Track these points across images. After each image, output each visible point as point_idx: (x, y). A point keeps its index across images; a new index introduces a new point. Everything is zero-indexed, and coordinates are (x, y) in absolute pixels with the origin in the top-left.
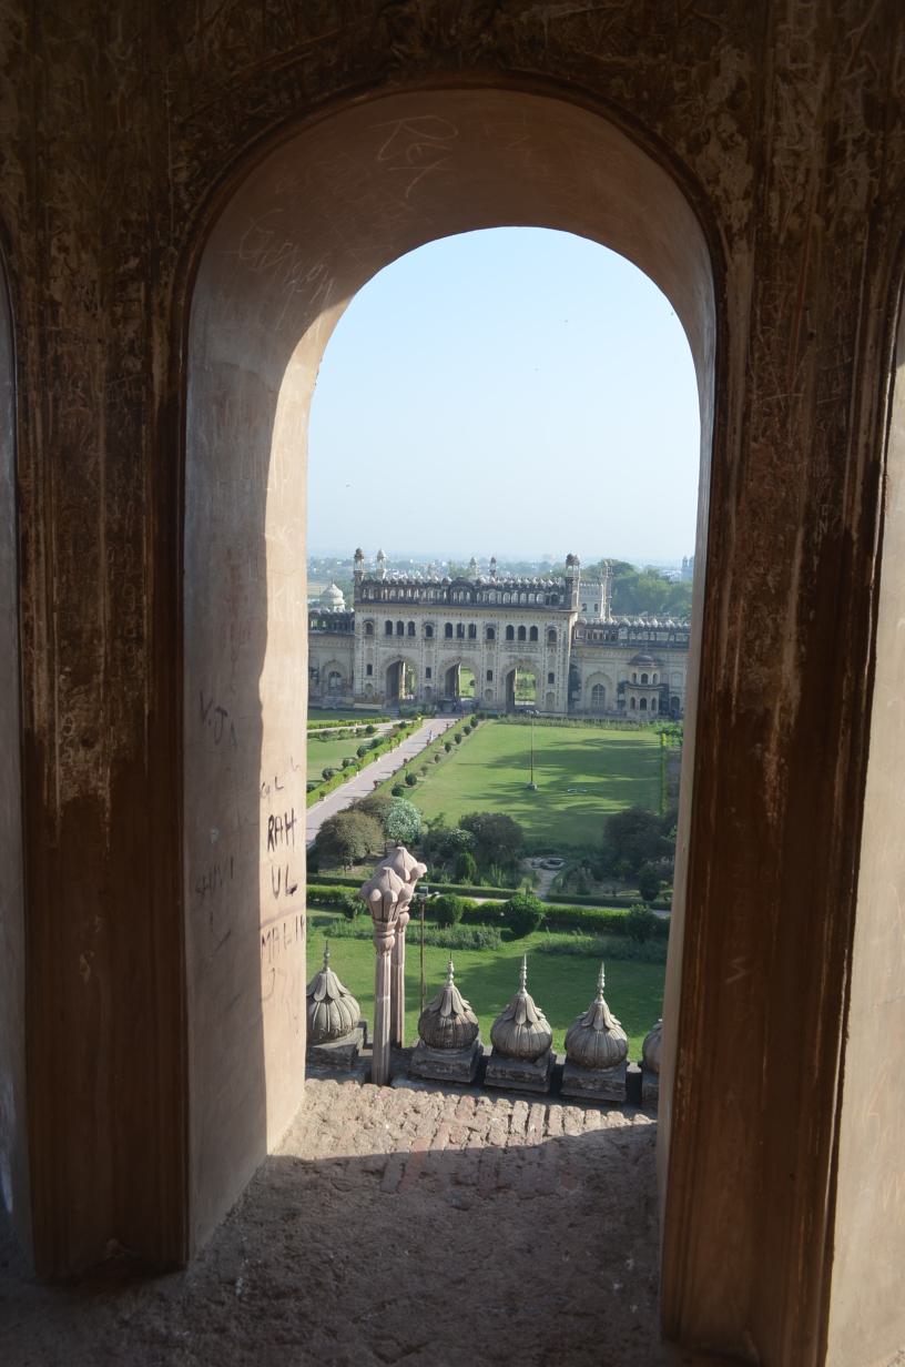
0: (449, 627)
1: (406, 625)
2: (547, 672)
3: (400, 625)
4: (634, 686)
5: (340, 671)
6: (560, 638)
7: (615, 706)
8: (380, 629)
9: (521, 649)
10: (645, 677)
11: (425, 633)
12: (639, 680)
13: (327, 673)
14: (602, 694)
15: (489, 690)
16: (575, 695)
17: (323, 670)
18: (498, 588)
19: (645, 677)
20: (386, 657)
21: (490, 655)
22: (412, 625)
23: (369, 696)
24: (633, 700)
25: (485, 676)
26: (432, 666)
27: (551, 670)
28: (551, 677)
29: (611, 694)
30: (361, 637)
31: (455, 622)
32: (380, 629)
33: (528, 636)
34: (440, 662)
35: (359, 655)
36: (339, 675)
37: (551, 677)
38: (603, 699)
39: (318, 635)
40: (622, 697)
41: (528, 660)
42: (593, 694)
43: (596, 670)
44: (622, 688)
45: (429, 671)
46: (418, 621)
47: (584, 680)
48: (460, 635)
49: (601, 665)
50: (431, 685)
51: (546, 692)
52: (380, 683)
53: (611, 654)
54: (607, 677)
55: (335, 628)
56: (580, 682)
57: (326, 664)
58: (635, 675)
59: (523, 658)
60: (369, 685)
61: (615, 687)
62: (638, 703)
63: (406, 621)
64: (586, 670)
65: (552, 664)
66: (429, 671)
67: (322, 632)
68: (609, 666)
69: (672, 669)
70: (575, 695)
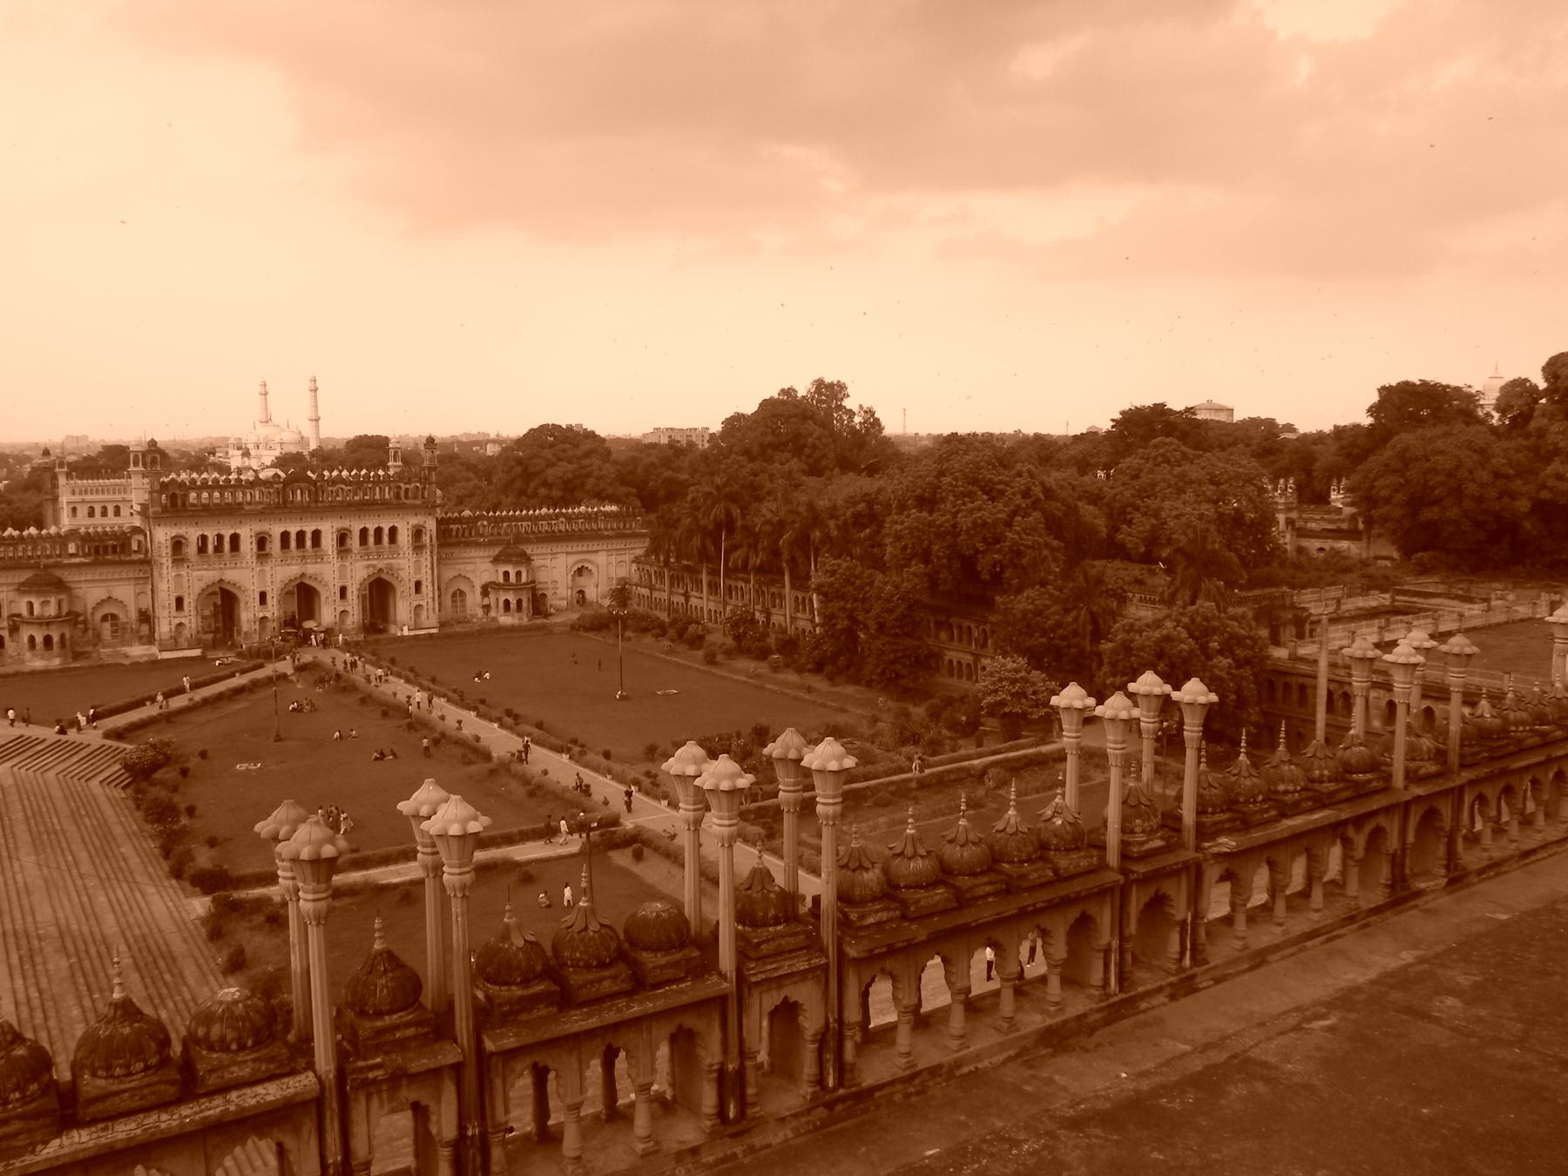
0: (285, 536)
1: (227, 539)
3: (220, 537)
4: (506, 585)
6: (426, 539)
7: (480, 612)
8: (191, 550)
9: (379, 555)
10: (519, 574)
12: (512, 578)
13: (98, 616)
14: (463, 601)
19: (519, 574)
20: (203, 585)
21: (342, 567)
22: (235, 539)
23: (182, 640)
24: (507, 602)
26: (268, 589)
27: (418, 577)
28: (418, 585)
29: (474, 600)
31: (293, 529)
32: (191, 550)
33: (386, 539)
34: (278, 585)
36: (114, 617)
37: (418, 585)
40: (486, 601)
41: (390, 568)
42: (454, 601)
44: (485, 591)
45: (263, 596)
46: (247, 533)
50: (268, 615)
52: (191, 620)
53: (474, 553)
55: (106, 552)
58: (506, 574)
60: (180, 624)
61: (478, 590)
62: (513, 605)
63: (227, 533)
65: (418, 570)
66: (263, 596)
68: (469, 567)
69: (537, 562)
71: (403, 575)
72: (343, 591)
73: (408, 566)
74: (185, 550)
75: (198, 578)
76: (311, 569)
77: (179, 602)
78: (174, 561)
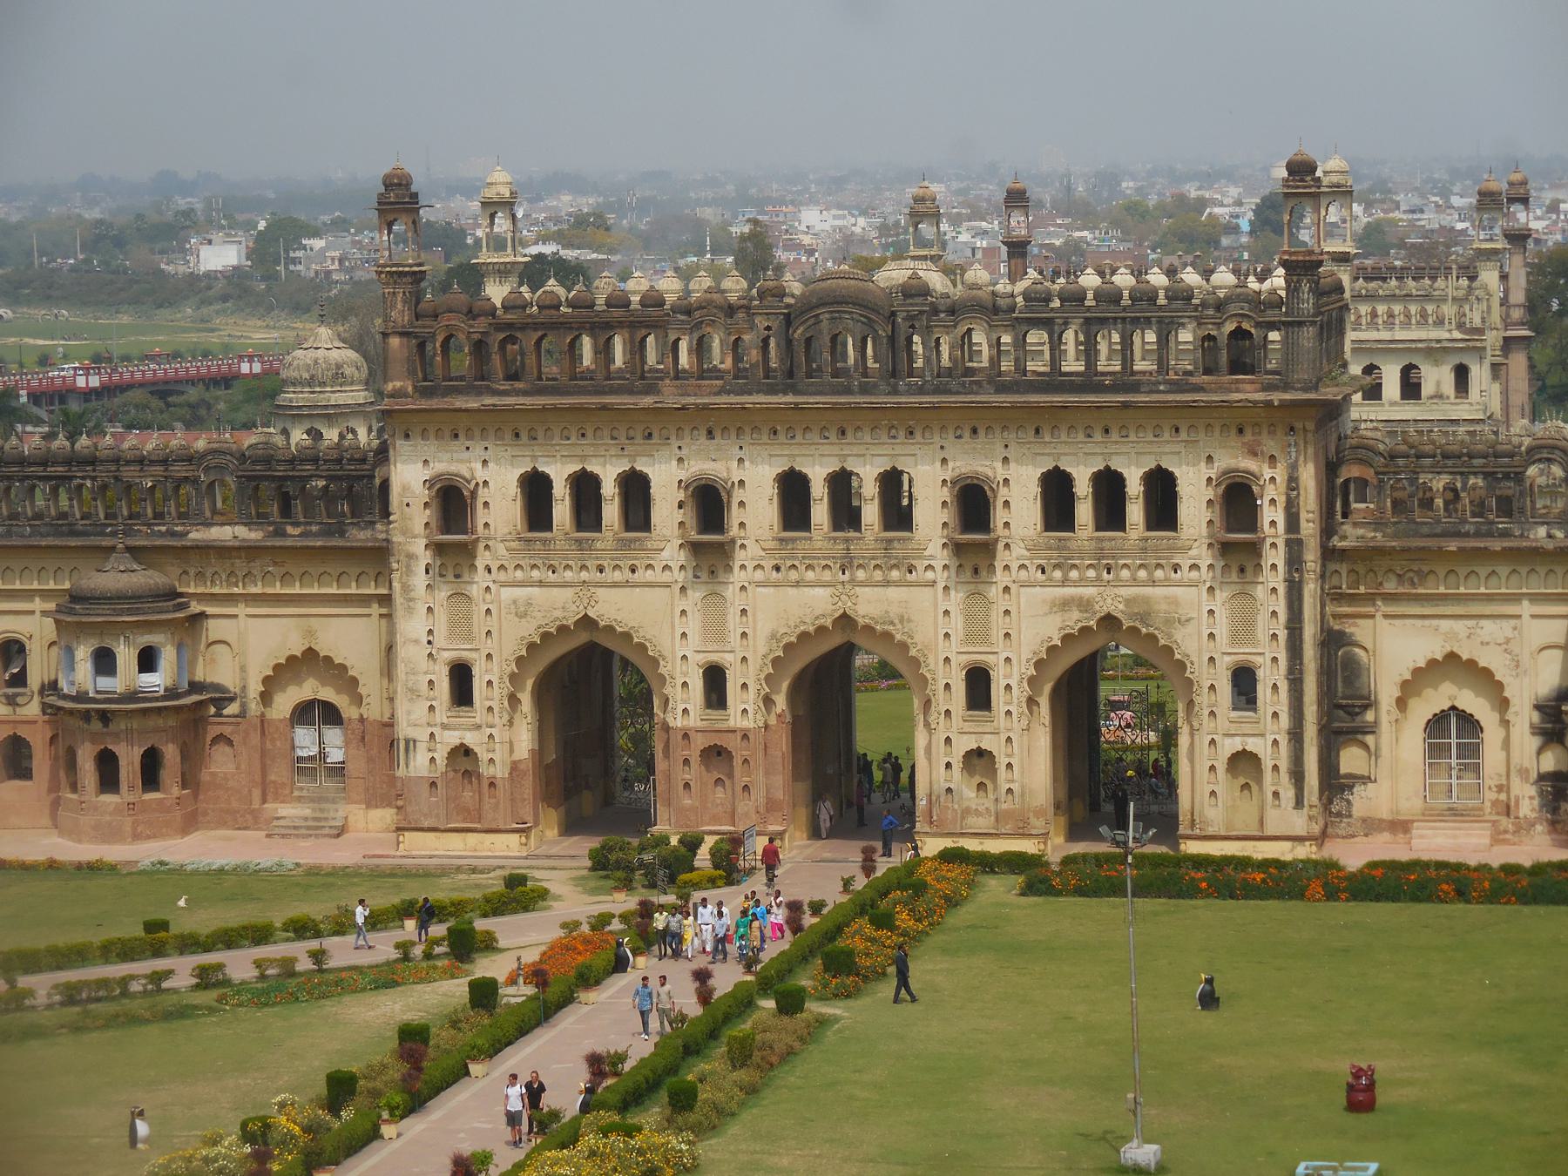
1: (609, 488)
2: (1225, 664)
5: (327, 694)
6: (1271, 515)
11: (689, 516)
15: (980, 753)
16: (1350, 760)
17: (266, 698)
18: (992, 310)
20: (529, 630)
25: (959, 689)
26: (726, 659)
27: (1244, 653)
28: (1244, 682)
30: (419, 547)
34: (760, 649)
35: (412, 626)
36: (331, 715)
37: (1244, 682)
38: (1477, 769)
39: (250, 551)
42: (1435, 751)
43: (1435, 649)
47: (1387, 693)
48: (846, 515)
49: (1460, 626)
51: (1231, 746)
54: (1487, 673)
56: (1369, 703)
57: (277, 667)
59: (1118, 609)
61: (1524, 717)
64: (1395, 645)
65: (1243, 629)
66: (715, 678)
67: (251, 535)
70: (1350, 760)
71: (1189, 643)
72: (979, 685)
73: (1205, 616)
74: (481, 517)
75: (517, 603)
76: (872, 603)
77: (461, 677)
78: (439, 549)
